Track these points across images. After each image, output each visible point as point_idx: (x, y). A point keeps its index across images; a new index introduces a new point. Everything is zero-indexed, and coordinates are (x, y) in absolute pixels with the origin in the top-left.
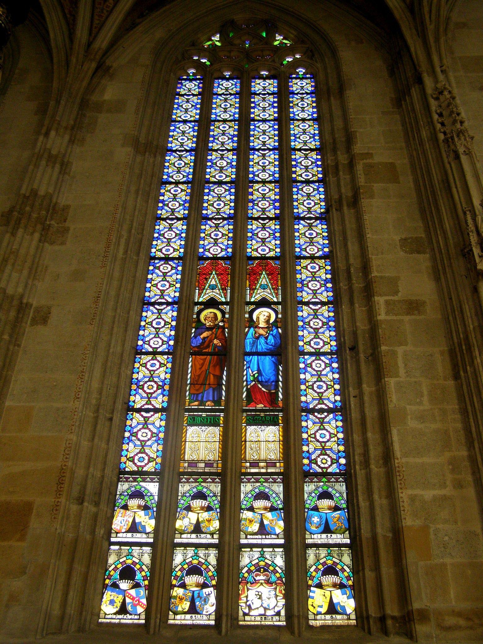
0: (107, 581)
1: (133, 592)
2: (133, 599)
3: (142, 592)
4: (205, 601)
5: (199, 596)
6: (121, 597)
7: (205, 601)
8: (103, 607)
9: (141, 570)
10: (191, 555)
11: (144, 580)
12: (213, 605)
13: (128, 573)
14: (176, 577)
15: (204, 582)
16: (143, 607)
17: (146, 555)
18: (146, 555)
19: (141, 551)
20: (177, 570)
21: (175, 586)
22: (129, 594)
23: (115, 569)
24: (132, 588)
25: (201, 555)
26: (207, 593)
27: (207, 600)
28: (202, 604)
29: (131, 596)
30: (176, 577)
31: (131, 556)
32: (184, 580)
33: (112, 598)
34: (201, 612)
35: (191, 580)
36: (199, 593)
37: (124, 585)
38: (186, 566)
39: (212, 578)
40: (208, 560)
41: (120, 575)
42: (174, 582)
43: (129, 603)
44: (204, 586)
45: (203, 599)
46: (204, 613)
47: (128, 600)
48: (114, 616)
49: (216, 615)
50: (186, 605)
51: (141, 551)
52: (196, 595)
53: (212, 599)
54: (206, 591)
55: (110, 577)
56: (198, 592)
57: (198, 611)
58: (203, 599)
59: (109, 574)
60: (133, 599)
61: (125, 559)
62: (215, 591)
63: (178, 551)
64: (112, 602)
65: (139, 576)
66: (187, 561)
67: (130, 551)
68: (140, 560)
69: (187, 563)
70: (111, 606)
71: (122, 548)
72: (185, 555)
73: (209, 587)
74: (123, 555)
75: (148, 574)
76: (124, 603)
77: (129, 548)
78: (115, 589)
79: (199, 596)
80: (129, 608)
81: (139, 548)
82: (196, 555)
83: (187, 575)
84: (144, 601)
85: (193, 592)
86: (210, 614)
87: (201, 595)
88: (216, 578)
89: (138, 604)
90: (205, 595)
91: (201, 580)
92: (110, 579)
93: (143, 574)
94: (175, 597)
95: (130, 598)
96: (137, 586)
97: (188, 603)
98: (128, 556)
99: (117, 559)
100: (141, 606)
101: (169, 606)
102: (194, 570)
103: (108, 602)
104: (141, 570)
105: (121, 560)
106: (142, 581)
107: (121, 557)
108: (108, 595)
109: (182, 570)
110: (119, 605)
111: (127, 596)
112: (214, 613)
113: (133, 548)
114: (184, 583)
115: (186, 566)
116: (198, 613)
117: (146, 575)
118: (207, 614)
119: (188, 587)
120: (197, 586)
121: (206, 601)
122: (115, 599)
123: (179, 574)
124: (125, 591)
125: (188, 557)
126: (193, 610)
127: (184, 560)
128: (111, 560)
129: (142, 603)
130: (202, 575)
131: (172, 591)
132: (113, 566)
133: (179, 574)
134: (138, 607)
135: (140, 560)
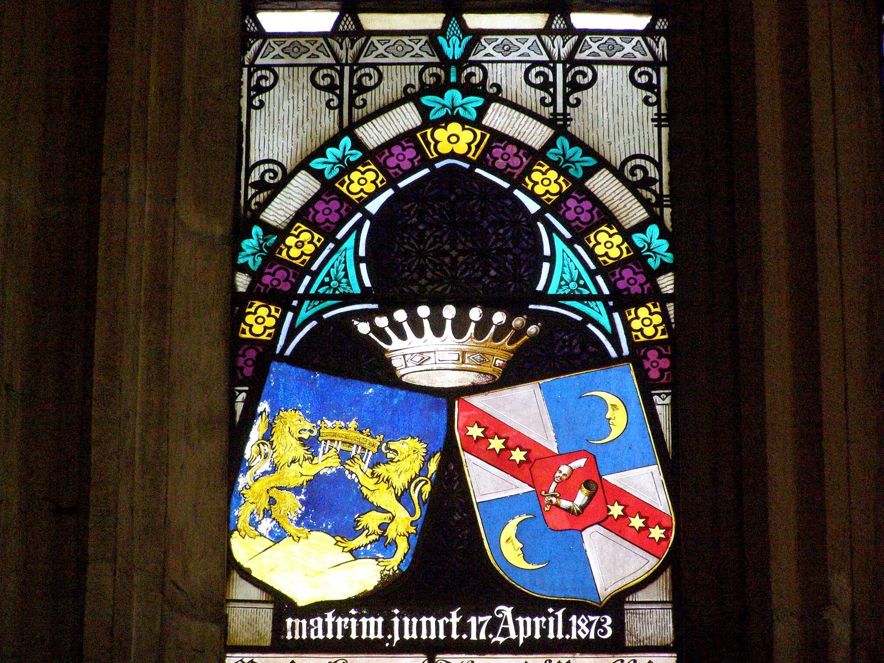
0: (259, 321)
1: (524, 409)
2: (533, 465)
3: (616, 407)
6: (409, 458)
8: (243, 548)
9: (585, 216)
11: (620, 302)
13: (455, 237)
16: (640, 539)
17: (613, 80)
18: (613, 80)
19: (560, 47)
22: (493, 427)
23: (327, 211)
24: (513, 374)
29: (513, 439)
31: (468, 90)
33: (326, 463)
37: (431, 353)
41: (377, 257)
43: (505, 507)
47: (485, 482)
48: (372, 627)
51: (560, 47)
55: (280, 285)
59: (270, 256)
60: (533, 465)
61: (407, 117)
64: (329, 506)
65: (562, 269)
67: (454, 48)
68: (559, 125)
70: (321, 541)
71: (372, 21)
74: (394, 82)
75: (656, 244)
76: (447, 513)
77: (433, 21)
78: (348, 389)
80: (509, 550)
81: (537, 21)
84: (647, 483)
89: (594, 514)
92: (282, 299)
93: (608, 244)
95: (501, 461)
96: (553, 352)
98: (439, 89)
99: (329, 123)
100: (618, 528)
103: (291, 504)
104: (585, 216)
105: (374, 134)
106: (598, 311)
107: (375, 99)
108: (284, 448)
110: (403, 524)
111: (478, 448)
113: (474, 21)
117: (638, 258)
122: (359, 472)
124: (450, 397)
128: (281, 126)
129: (633, 505)
132: (303, 187)
134: (595, 540)
135: (559, 125)
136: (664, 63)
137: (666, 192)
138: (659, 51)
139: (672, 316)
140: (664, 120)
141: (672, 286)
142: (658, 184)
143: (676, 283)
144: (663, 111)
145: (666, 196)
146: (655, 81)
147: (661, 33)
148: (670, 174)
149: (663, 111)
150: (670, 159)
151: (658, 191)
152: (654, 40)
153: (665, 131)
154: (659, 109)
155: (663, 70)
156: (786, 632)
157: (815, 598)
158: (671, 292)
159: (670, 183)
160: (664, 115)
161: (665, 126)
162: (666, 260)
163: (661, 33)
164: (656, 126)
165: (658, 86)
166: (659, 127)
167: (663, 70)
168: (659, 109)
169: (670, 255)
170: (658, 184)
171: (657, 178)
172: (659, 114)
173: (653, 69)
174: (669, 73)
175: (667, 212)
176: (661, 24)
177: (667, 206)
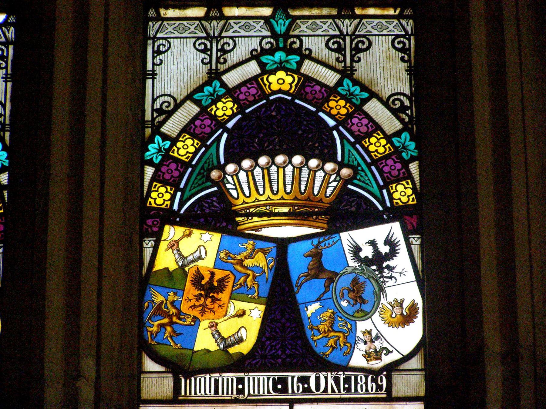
4: (356, 291)
5: (317, 269)
7: (356, 291)
10: (255, 44)
12: (407, 319)
14: (170, 171)
15: (344, 192)
20: (172, 127)
21: (169, 217)
25: (316, 45)
26: (367, 252)
27: (368, 293)
28: (337, 312)
30: (170, 171)
32: (221, 183)
34: (335, 357)
35: (260, 182)
36: (316, 255)
38: (224, 108)
39: (392, 168)
40: (362, 71)
42: (160, 196)
44: (345, 211)
45: (344, 282)
46: (358, 360)
49: (430, 372)
50: (244, 322)
52: (298, 262)
53: (403, 286)
54: (366, 237)
56: (307, 246)
57: (319, 349)
58: (344, 282)
62: (416, 241)
63: (170, 27)
66: (232, 79)
69: (231, 92)
72: (214, 48)
73: (372, 218)
79: (317, 269)
82: (284, 43)
83: (234, 157)
85: (282, 245)
86: (391, 368)
87: (328, 263)
88: (414, 167)
90: (352, 263)
91: (323, 179)
94: (172, 279)
97: (255, 313)
101: (141, 326)
102: (276, 126)
109: (202, 127)
112: (416, 363)
114: (222, 194)
115: (224, 108)
116: (322, 364)
118: (377, 365)
119: (247, 224)
120: (298, 215)
121: (363, 293)
123: (186, 148)
125: (232, 58)
126: (287, 344)
127: (214, 75)
130: (327, 155)
131: (148, 244)
133: (186, 148)
136: (11, 43)
137: (7, 122)
138: (9, 35)
139: (6, 199)
140: (9, 78)
141: (7, 181)
142: (3, 117)
143: (9, 179)
144: (9, 72)
145: (7, 125)
146: (5, 54)
147: (11, 24)
148: (11, 111)
149: (9, 72)
150: (12, 101)
151: (3, 122)
152: (7, 29)
153: (9, 85)
154: (7, 71)
155: (11, 47)
156: (53, 394)
157: (73, 374)
158: (7, 184)
159: (11, 115)
160: (9, 74)
161: (9, 81)
162: (4, 164)
163: (11, 24)
164: (4, 81)
165: (7, 57)
166: (6, 82)
167: (11, 47)
168: (7, 71)
169: (7, 161)
170: (3, 117)
171: (3, 113)
172: (6, 74)
173: (5, 46)
174: (14, 49)
175: (7, 134)
176: (12, 19)
177: (7, 131)
